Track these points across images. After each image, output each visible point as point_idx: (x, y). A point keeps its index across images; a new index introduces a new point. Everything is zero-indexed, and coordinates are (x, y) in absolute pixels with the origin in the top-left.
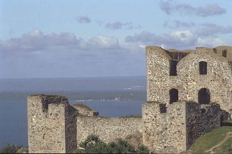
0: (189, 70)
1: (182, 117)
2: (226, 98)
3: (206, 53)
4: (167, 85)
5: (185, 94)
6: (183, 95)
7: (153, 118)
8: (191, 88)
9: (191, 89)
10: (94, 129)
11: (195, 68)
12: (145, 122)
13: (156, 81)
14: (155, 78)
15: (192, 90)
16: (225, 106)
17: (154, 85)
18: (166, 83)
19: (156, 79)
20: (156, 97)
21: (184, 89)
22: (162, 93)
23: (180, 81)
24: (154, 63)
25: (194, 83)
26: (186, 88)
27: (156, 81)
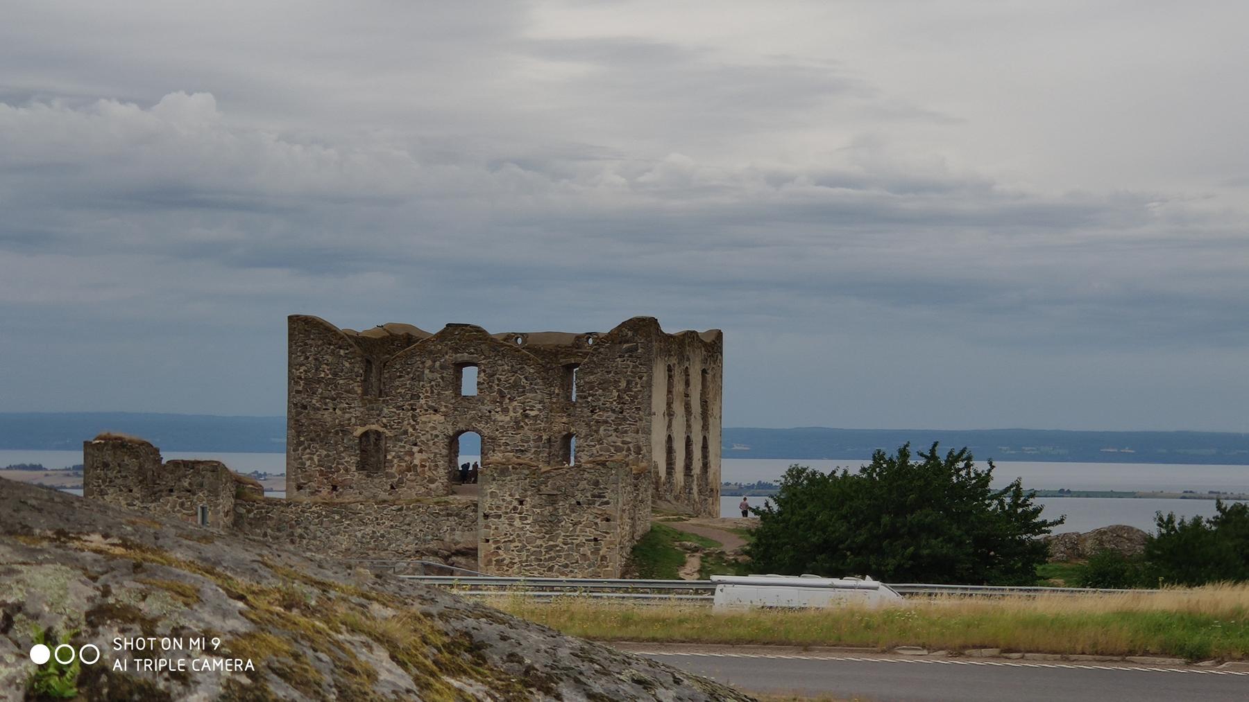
1: (607, 503)
4: (353, 420)
7: (515, 503)
10: (292, 535)
11: (442, 378)
12: (486, 516)
13: (318, 409)
18: (347, 416)
21: (406, 432)
22: (336, 443)
25: (439, 418)
26: (411, 430)
27: (318, 409)
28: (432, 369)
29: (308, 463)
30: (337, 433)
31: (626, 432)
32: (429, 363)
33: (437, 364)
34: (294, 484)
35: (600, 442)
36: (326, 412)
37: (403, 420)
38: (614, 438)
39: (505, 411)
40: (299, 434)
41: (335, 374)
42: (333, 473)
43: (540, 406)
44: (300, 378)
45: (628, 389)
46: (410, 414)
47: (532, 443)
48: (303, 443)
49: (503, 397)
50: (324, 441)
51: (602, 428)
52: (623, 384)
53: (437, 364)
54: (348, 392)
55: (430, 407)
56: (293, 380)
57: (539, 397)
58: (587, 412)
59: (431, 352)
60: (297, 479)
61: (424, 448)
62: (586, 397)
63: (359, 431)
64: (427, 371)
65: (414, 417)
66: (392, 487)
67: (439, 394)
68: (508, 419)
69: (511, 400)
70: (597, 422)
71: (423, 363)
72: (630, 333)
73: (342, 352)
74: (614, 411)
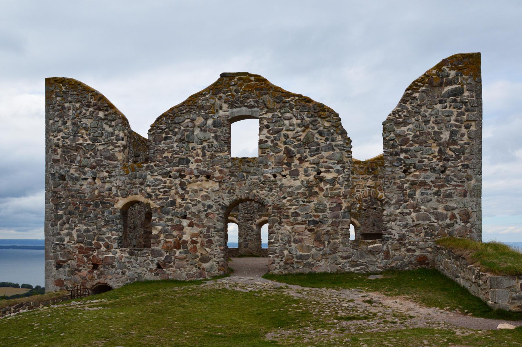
0: (191, 145)
2: (329, 229)
3: (257, 89)
5: (175, 220)
6: (171, 220)
8: (199, 199)
9: (199, 202)
11: (216, 138)
13: (77, 179)
14: (72, 171)
15: (204, 205)
16: (324, 255)
17: (69, 190)
18: (107, 186)
19: (76, 174)
20: (76, 226)
21: (173, 203)
22: (96, 217)
23: (159, 177)
24: (71, 127)
25: (212, 185)
26: (179, 200)
27: (75, 179)
28: (203, 128)
29: (67, 239)
30: (96, 205)
31: (450, 195)
32: (200, 121)
33: (210, 122)
34: (52, 262)
35: (416, 208)
36: (85, 183)
37: (170, 188)
38: (434, 203)
39: (295, 174)
40: (57, 206)
41: (94, 140)
42: (93, 250)
43: (338, 167)
44: (57, 145)
45: (452, 141)
46: (178, 181)
47: (328, 213)
48: (61, 217)
49: (290, 155)
50: (83, 216)
51: (418, 192)
52: (445, 136)
53: (210, 122)
54: (108, 158)
55: (202, 173)
56: (50, 147)
57: (338, 156)
58: (399, 172)
59: (202, 107)
60: (55, 257)
61: (195, 220)
62: (397, 154)
63: (121, 203)
64: (197, 131)
65: (183, 185)
66: (159, 266)
67: (212, 156)
68: (298, 183)
69: (302, 160)
70: (413, 184)
71: (192, 120)
72: (453, 73)
73: (101, 114)
74: (433, 170)
